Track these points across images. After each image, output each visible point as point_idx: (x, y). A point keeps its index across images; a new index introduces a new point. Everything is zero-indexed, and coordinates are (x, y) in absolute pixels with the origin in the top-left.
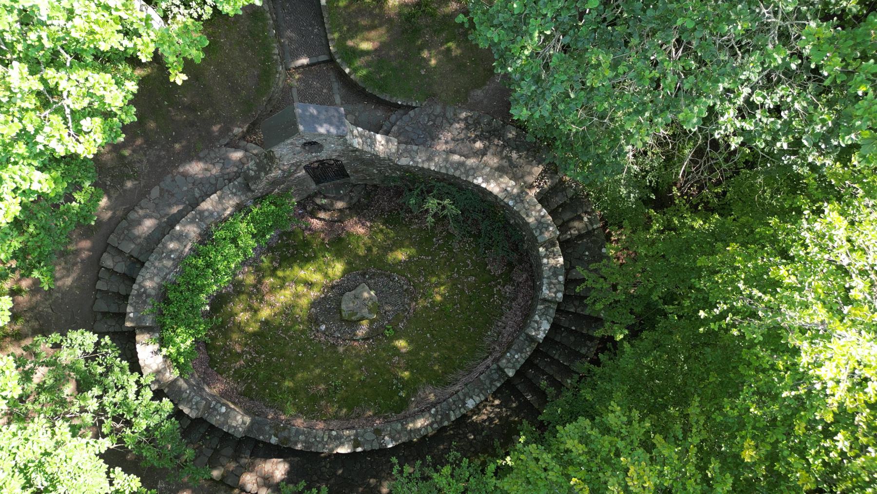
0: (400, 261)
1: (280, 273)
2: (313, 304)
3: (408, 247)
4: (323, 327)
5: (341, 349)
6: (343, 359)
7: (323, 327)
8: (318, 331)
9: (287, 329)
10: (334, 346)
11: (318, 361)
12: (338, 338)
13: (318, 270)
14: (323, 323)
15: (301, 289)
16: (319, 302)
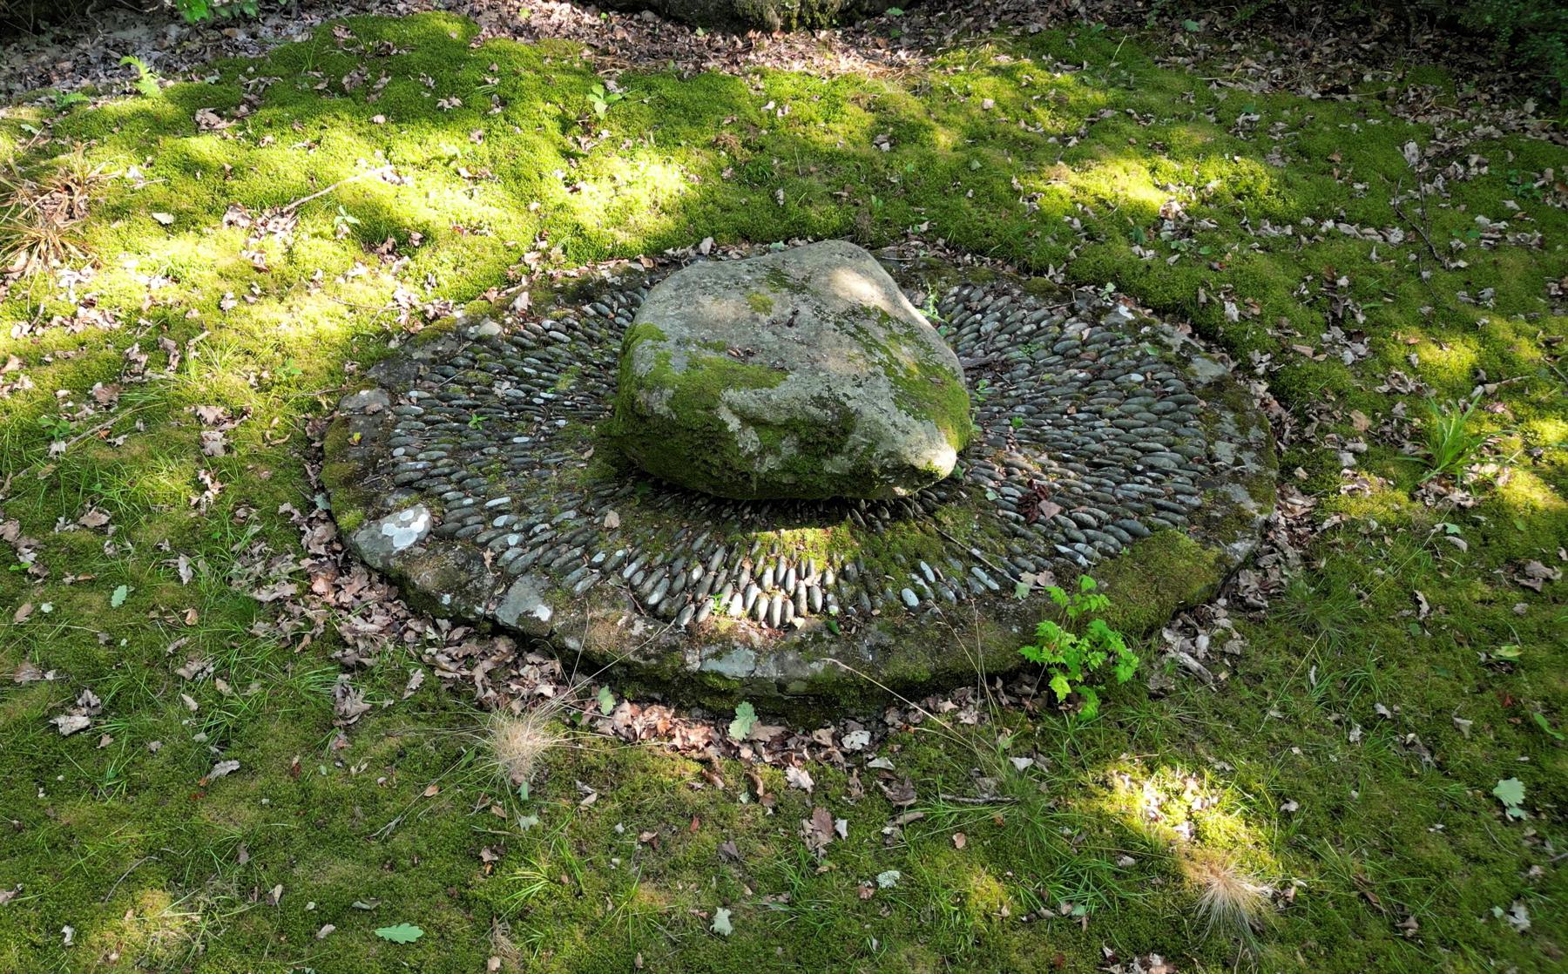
0: (1158, 221)
1: (204, 146)
2: (382, 356)
3: (1202, 153)
4: (407, 527)
5: (523, 741)
6: (511, 849)
7: (407, 527)
8: (345, 558)
9: (72, 488)
10: (461, 707)
11: (230, 818)
12: (527, 639)
13: (518, 179)
14: (417, 489)
15: (321, 247)
16: (440, 362)
